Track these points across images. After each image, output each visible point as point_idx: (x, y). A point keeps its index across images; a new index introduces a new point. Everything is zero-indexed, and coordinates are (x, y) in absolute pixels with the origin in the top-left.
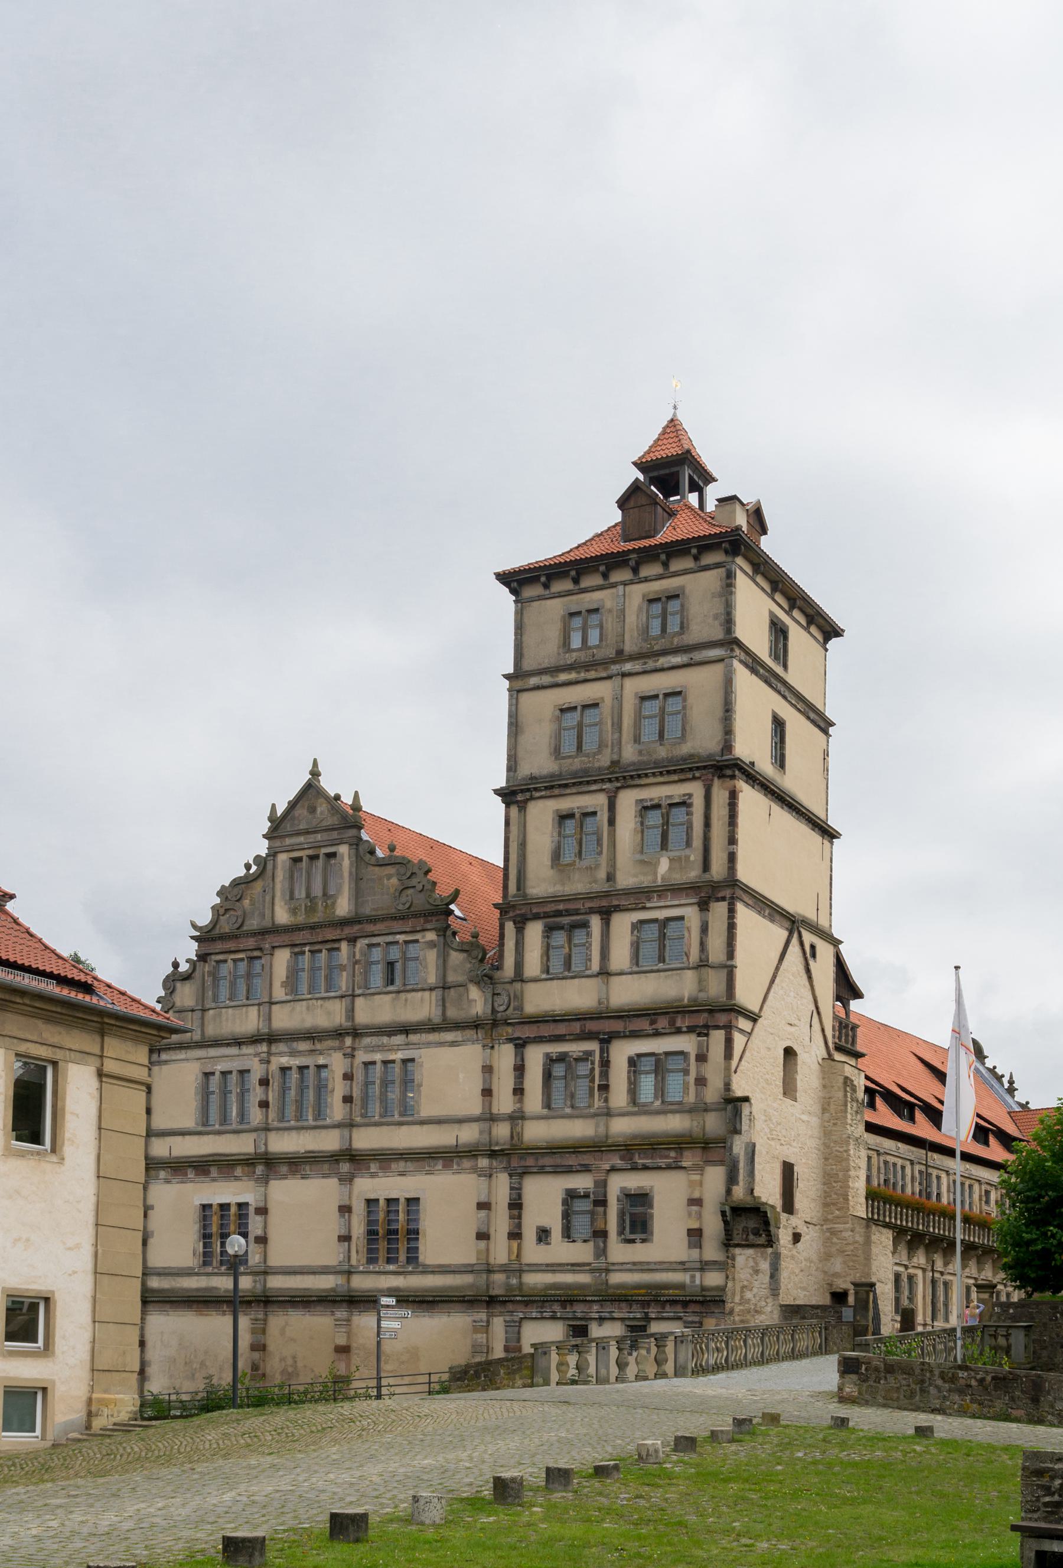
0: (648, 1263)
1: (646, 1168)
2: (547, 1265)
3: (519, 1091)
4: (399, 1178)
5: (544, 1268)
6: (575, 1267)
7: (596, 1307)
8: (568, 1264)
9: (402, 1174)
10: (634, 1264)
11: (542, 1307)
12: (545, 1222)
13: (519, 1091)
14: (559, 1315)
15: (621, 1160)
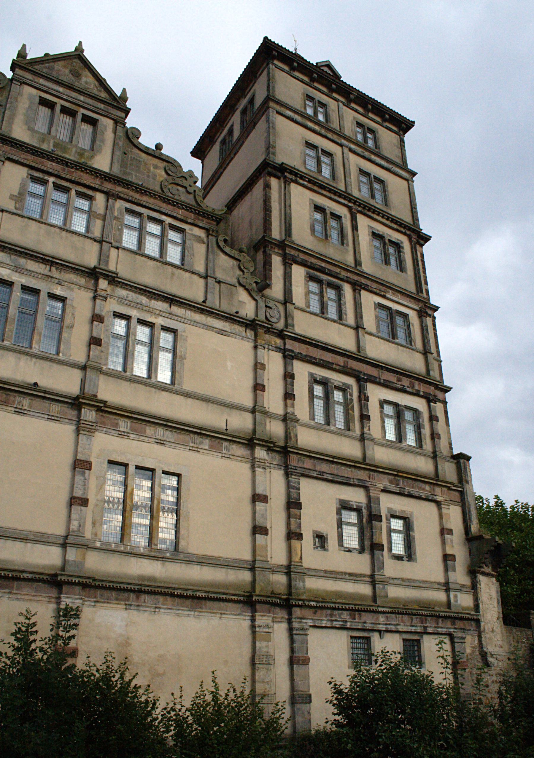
0: (414, 581)
1: (410, 496)
2: (326, 572)
3: (289, 396)
4: (156, 446)
5: (322, 574)
6: (353, 577)
7: (382, 619)
8: (345, 573)
9: (161, 443)
10: (403, 580)
11: (331, 615)
12: (322, 529)
13: (289, 396)
14: (348, 625)
15: (391, 482)
